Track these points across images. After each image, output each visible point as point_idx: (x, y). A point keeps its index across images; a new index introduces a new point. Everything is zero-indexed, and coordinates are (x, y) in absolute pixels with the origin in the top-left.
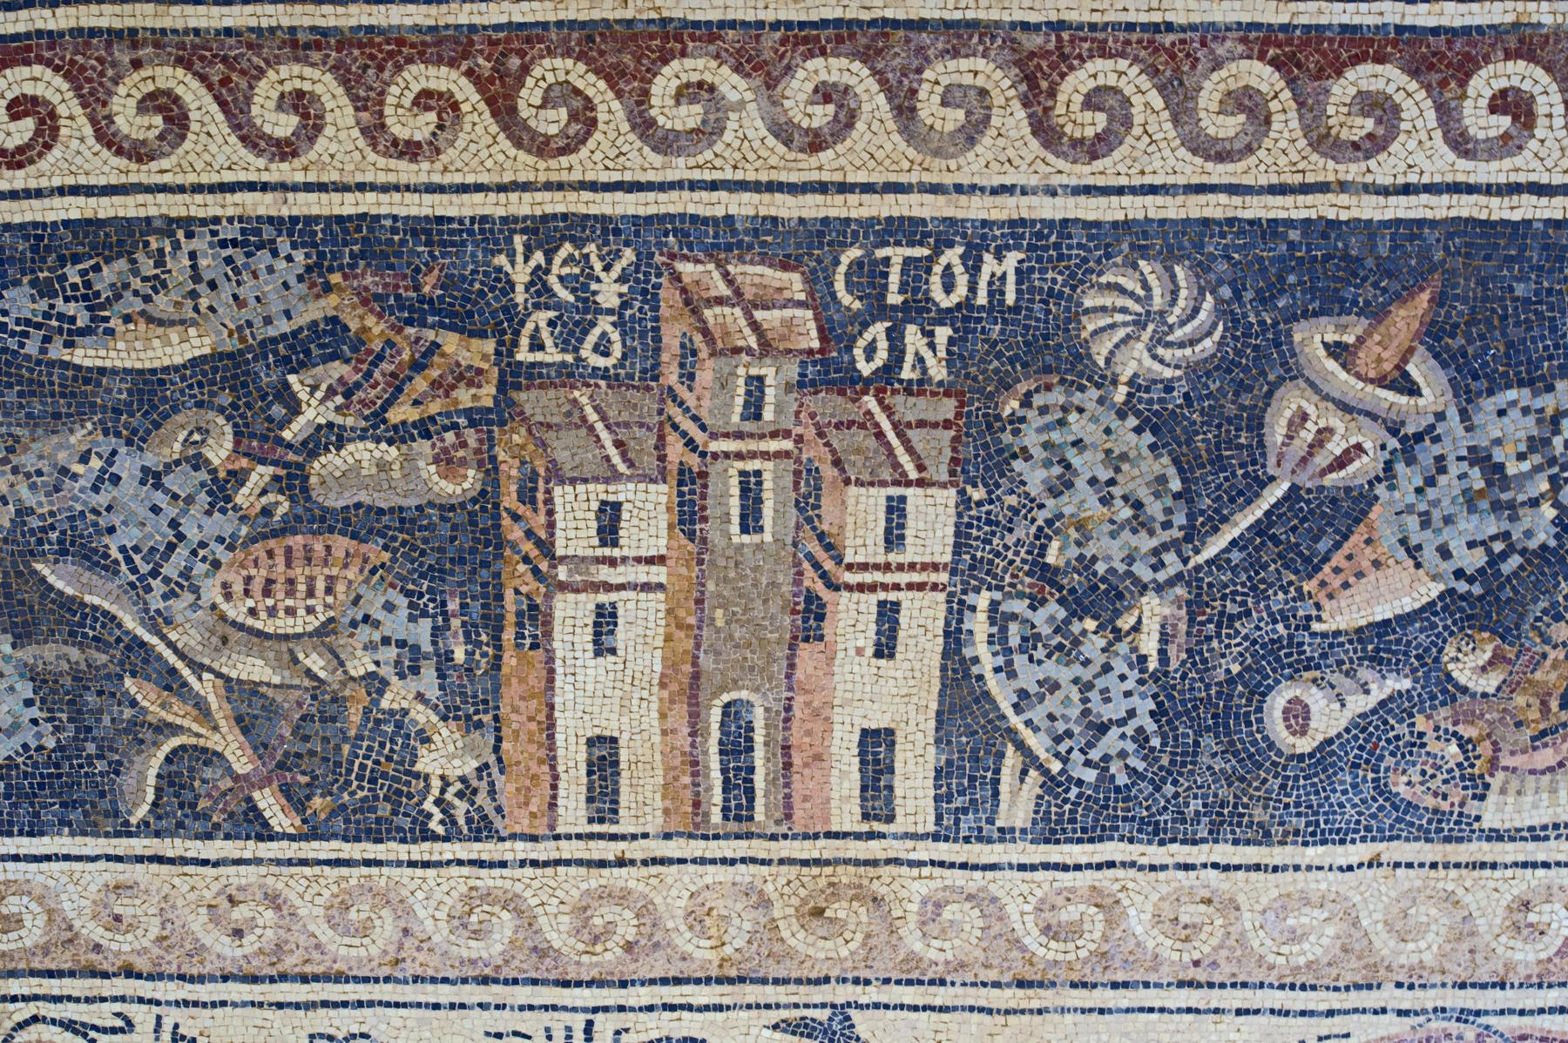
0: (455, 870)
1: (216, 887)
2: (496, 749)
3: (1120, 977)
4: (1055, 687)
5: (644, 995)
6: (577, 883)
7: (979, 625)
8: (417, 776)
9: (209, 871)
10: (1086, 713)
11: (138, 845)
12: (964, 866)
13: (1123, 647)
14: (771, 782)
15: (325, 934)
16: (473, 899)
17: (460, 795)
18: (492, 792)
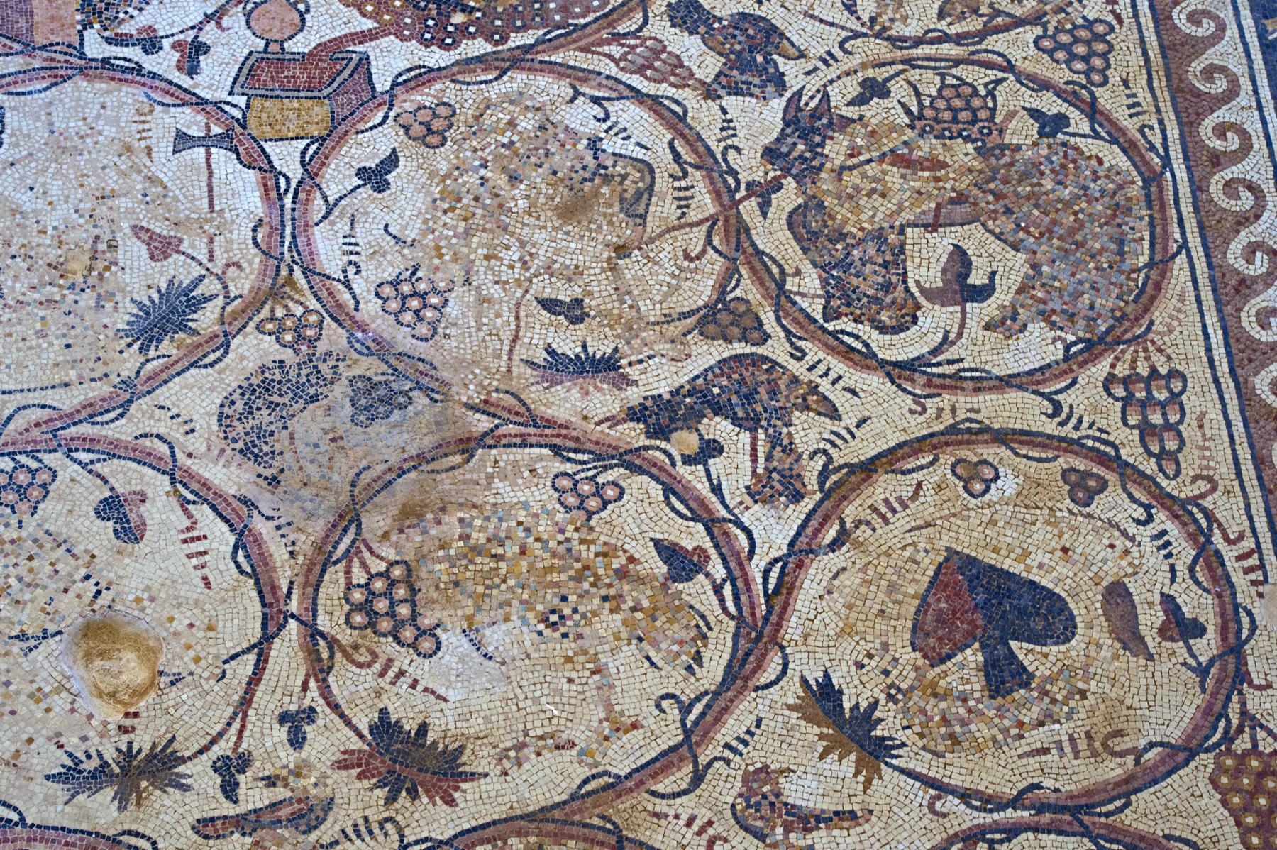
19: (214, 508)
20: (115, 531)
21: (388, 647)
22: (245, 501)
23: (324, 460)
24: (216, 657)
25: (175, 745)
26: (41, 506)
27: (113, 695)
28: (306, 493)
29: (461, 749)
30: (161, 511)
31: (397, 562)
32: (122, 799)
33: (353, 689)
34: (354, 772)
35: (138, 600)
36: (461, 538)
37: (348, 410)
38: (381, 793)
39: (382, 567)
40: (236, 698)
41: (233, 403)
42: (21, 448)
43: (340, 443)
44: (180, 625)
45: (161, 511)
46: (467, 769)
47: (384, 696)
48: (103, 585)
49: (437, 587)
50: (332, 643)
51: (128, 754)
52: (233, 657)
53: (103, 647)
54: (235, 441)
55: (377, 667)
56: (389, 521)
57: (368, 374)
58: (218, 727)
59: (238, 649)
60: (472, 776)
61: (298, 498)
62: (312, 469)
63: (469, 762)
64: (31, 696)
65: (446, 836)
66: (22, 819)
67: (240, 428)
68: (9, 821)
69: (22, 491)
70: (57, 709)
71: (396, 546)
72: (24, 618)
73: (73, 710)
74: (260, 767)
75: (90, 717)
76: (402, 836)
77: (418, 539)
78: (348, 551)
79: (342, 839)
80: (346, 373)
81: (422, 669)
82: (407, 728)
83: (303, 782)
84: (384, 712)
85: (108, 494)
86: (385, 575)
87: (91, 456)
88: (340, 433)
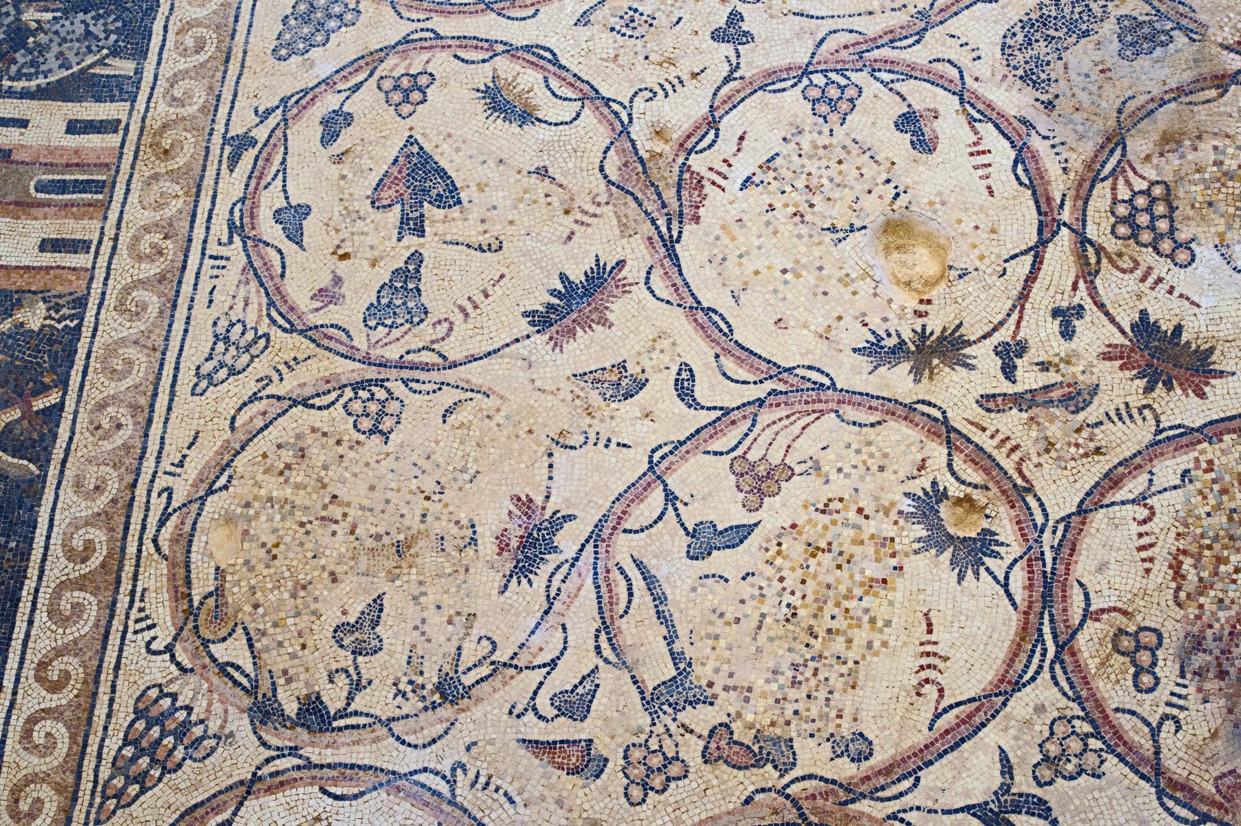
0: (102, 317)
1: (87, 434)
2: (35, 293)
3: (232, 19)
4: (61, 54)
5: (199, 233)
6: (123, 259)
7: (18, 85)
8: (41, 330)
9: (77, 437)
10: (78, 40)
11: (53, 471)
12: (153, 89)
13: (46, 26)
14: (85, 172)
15: (128, 382)
16: (121, 308)
17: (57, 312)
18: (60, 296)
19: (997, 126)
20: (912, 142)
21: (1147, 257)
22: (1024, 122)
23: (1094, 89)
24: (998, 256)
25: (962, 330)
26: (849, 118)
27: (908, 284)
28: (1078, 117)
29: (1211, 350)
30: (951, 126)
31: (1158, 182)
32: (917, 372)
33: (1117, 291)
34: (1118, 363)
35: (931, 203)
36: (1215, 163)
37: (1116, 46)
38: (1141, 383)
39: (1144, 186)
40: (1015, 293)
41: (1014, 35)
42: (832, 66)
43: (1108, 74)
44: (967, 227)
45: (951, 126)
46: (1217, 367)
47: (1144, 299)
48: (901, 189)
49: (1193, 206)
50: (1099, 250)
51: (923, 335)
52: (1013, 257)
53: (900, 242)
54: (1016, 68)
55: (1139, 273)
56: (1151, 145)
57: (1134, 14)
58: (1000, 317)
59: (1017, 251)
60: (1221, 374)
61: (1071, 121)
62: (1083, 97)
63: (1219, 361)
64: (840, 280)
65: (1197, 425)
66: (833, 384)
67: (1020, 57)
68: (822, 385)
69: (833, 104)
70: (862, 293)
71: (1157, 167)
72: (834, 214)
73: (875, 295)
74: (1033, 355)
75: (890, 301)
76: (1158, 422)
77: (1177, 162)
78: (1114, 170)
79: (1106, 420)
80: (1115, 12)
81: (1177, 277)
82: (1164, 328)
83: (1072, 369)
84: (1144, 313)
85: (906, 110)
86: (1147, 193)
87: (892, 76)
88: (1109, 65)
